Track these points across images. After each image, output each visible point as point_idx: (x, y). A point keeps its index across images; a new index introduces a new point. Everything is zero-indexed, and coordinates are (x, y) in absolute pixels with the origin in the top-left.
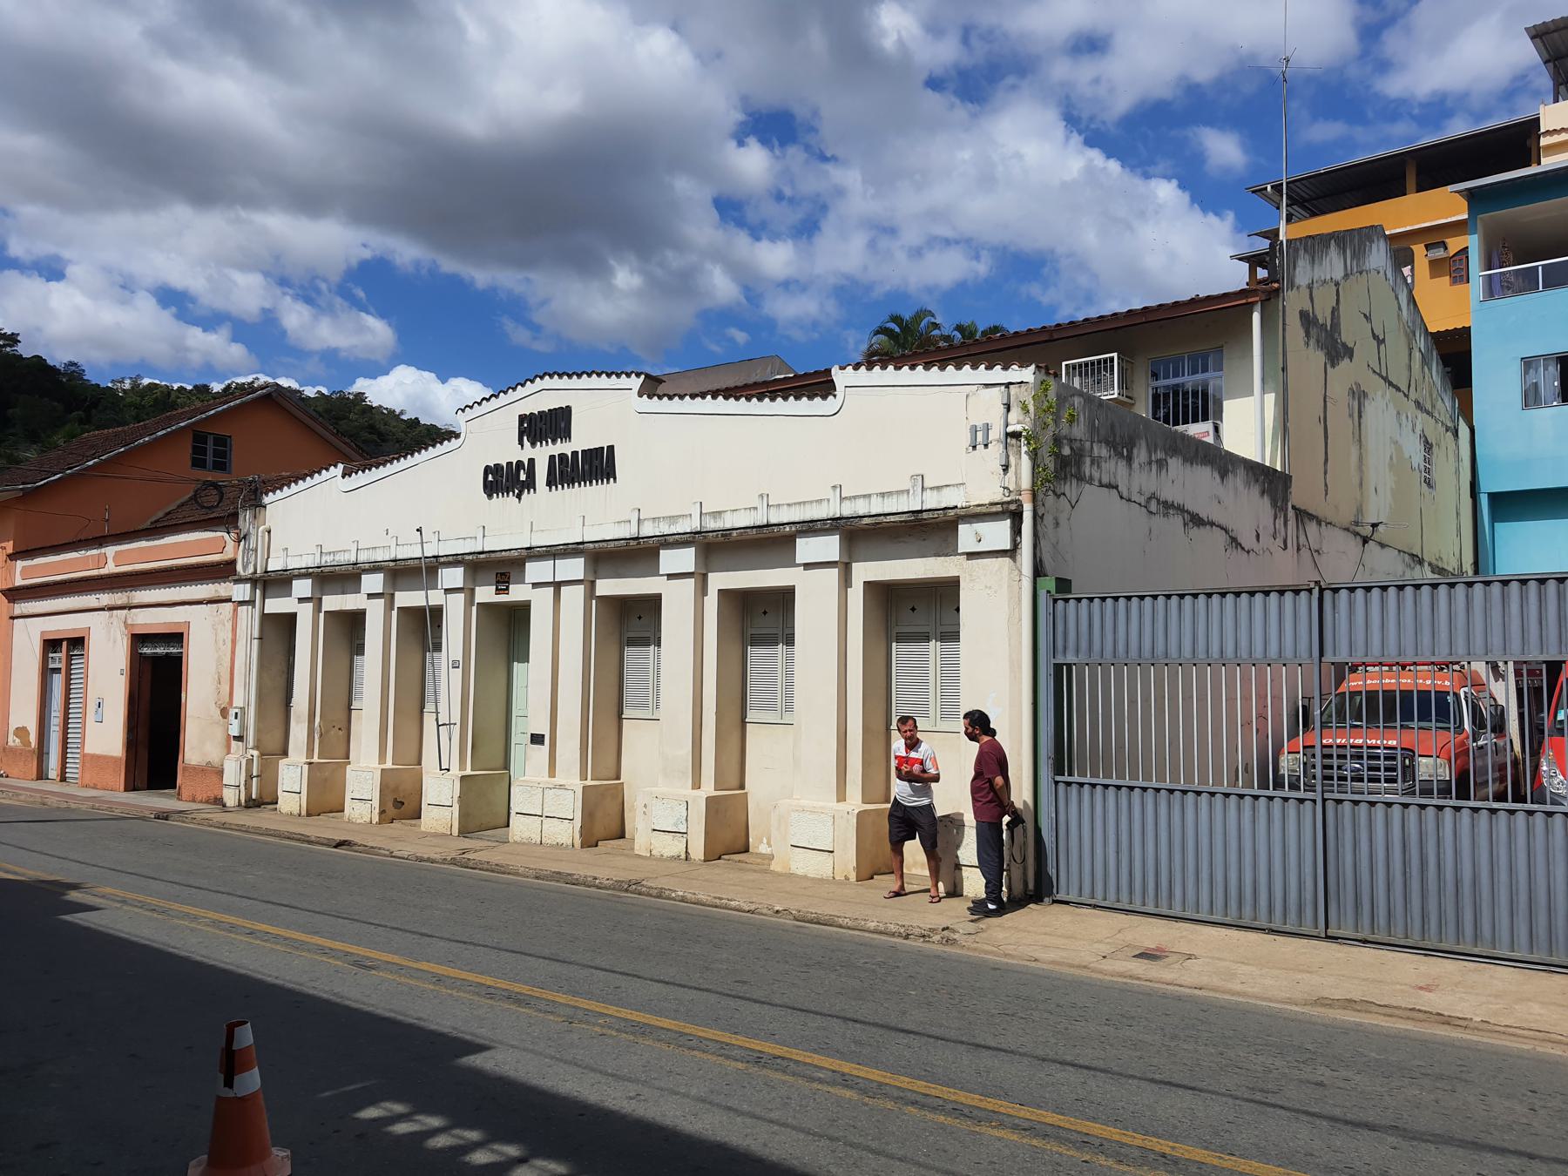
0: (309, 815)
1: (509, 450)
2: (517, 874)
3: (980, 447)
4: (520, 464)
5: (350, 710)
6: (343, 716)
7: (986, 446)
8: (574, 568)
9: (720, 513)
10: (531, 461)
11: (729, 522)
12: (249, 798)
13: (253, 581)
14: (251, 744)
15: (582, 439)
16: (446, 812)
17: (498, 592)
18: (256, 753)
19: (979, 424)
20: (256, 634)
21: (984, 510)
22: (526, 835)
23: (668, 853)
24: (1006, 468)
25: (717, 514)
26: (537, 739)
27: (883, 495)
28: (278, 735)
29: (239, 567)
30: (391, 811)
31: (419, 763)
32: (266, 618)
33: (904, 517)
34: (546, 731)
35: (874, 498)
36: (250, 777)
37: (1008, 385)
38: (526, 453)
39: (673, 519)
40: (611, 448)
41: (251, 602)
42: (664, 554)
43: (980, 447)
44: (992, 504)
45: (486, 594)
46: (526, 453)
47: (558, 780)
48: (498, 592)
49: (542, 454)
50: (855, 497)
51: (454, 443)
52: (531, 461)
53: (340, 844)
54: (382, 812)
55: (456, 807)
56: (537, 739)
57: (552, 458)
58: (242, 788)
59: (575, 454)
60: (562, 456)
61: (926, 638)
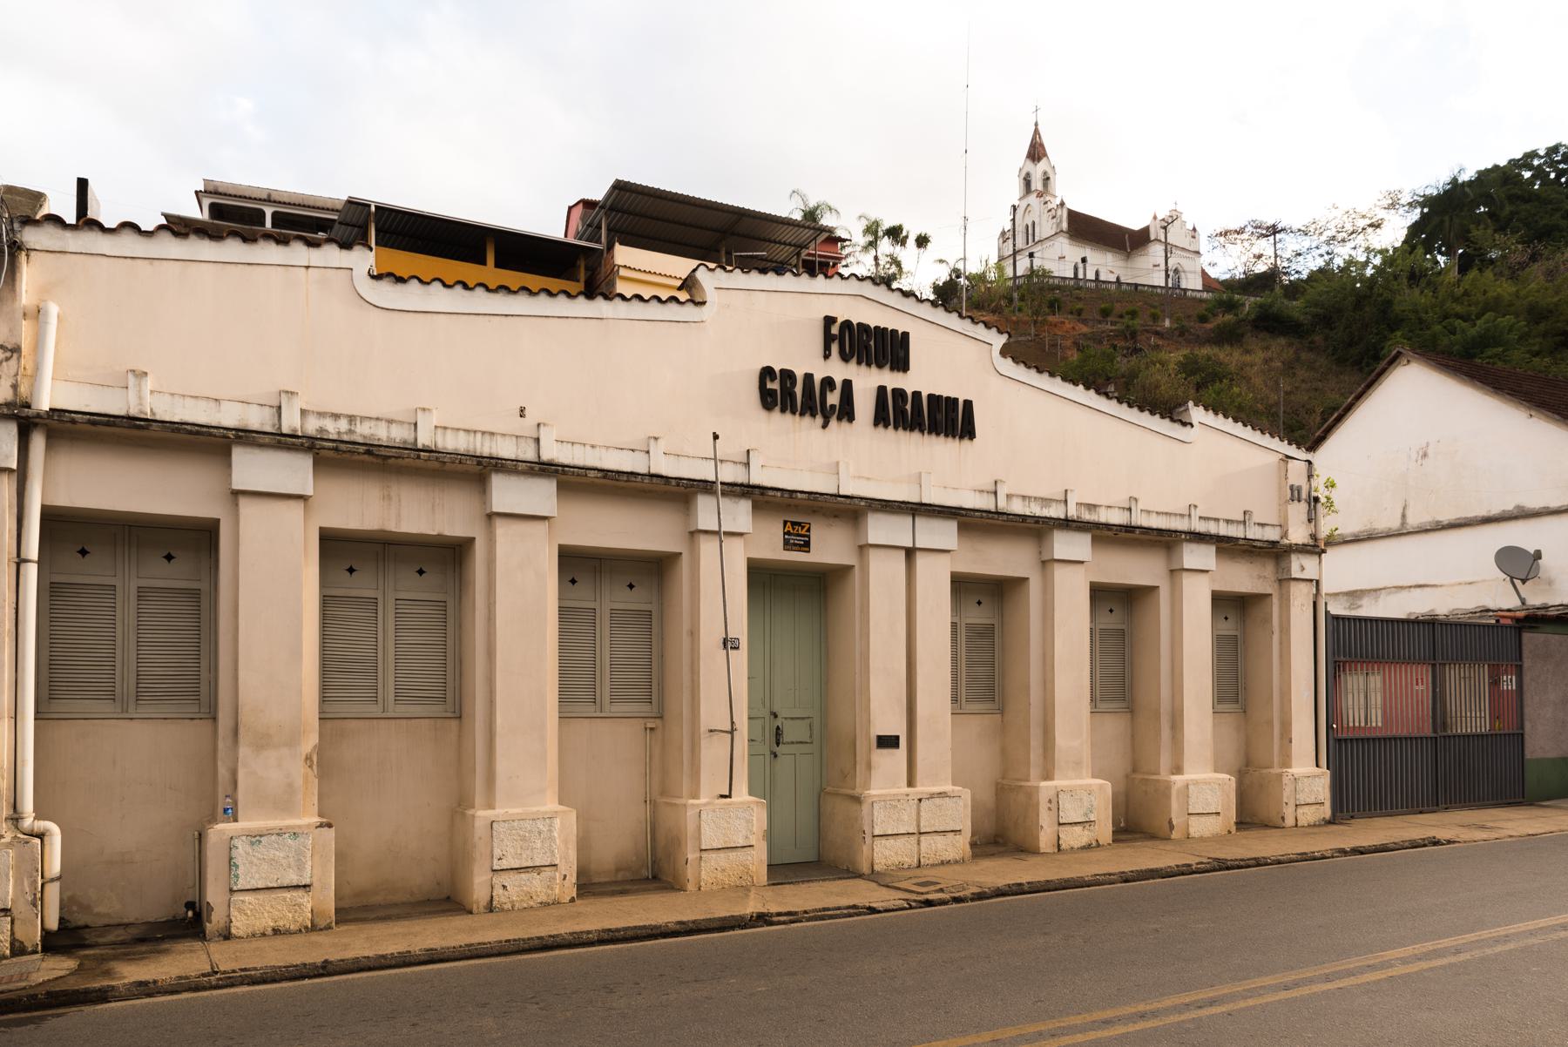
4: (828, 383)
10: (847, 384)
15: (926, 375)
17: (788, 545)
24: (1310, 521)
25: (1092, 507)
27: (1228, 521)
38: (838, 370)
39: (1046, 501)
40: (968, 404)
45: (769, 544)
48: (788, 545)
49: (867, 381)
57: (882, 390)
59: (917, 395)
60: (899, 394)
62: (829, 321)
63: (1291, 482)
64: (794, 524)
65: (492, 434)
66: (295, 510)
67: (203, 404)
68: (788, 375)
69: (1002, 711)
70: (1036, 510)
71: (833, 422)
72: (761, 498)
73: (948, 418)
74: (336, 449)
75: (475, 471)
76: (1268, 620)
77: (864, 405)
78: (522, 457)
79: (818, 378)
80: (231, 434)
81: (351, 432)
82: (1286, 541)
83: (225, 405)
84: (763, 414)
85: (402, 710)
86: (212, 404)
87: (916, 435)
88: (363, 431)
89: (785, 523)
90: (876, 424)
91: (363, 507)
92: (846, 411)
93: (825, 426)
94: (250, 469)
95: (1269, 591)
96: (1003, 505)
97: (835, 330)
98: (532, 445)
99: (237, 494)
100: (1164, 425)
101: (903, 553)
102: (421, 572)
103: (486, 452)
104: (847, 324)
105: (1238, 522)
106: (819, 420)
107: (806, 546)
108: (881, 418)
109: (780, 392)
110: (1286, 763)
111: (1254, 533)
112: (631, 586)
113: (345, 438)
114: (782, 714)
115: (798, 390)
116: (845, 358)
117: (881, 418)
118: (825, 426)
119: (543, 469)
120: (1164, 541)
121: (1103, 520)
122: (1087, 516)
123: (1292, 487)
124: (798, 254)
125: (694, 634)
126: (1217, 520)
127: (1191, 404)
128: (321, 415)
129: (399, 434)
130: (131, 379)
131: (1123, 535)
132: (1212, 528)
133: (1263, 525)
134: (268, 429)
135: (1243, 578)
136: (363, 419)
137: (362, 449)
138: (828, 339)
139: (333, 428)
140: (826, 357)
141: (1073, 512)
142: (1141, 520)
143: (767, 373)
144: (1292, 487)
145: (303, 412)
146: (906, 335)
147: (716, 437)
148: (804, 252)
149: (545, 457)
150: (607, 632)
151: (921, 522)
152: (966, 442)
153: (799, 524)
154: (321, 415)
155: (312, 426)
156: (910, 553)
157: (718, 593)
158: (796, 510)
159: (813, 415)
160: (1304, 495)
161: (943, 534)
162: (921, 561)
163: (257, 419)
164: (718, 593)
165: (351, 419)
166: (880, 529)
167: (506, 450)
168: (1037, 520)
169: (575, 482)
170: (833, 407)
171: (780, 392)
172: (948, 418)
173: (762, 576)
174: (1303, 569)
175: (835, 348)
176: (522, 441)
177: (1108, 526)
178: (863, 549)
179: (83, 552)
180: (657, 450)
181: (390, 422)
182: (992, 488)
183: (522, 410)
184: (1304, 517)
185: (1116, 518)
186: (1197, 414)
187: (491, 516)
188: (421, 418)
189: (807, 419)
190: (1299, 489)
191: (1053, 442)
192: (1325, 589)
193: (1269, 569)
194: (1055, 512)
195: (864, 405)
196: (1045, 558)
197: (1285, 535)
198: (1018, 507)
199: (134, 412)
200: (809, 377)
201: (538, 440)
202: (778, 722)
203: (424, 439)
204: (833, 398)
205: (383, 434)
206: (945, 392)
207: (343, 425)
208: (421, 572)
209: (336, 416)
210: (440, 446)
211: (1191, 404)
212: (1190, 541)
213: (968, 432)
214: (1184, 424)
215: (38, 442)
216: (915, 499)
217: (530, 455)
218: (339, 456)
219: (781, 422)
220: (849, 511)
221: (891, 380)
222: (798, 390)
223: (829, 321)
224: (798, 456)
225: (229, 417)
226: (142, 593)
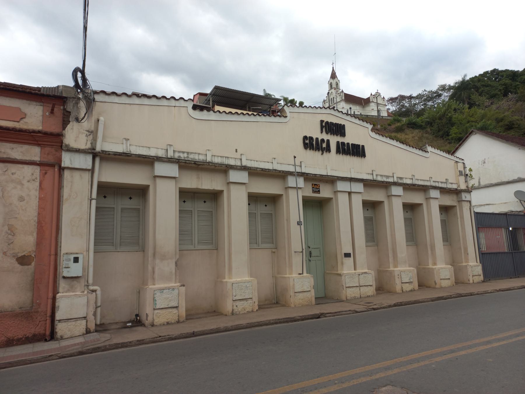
0: (187, 319)
4: (323, 140)
10: (328, 141)
13: (95, 154)
17: (314, 192)
22: (353, 295)
24: (466, 182)
25: (401, 178)
26: (347, 255)
27: (442, 182)
34: (350, 251)
38: (325, 137)
39: (388, 177)
40: (363, 146)
45: (309, 193)
49: (334, 140)
51: (282, 119)
55: (313, 292)
56: (347, 255)
58: (91, 317)
59: (348, 144)
60: (343, 143)
62: (322, 121)
64: (315, 185)
65: (228, 157)
66: (173, 182)
67: (145, 149)
68: (311, 138)
69: (377, 245)
70: (385, 179)
71: (325, 153)
72: (307, 177)
73: (358, 151)
74: (185, 163)
75: (224, 169)
76: (456, 214)
78: (237, 165)
79: (320, 139)
80: (155, 158)
81: (188, 157)
82: (459, 188)
83: (152, 149)
84: (304, 150)
85: (200, 247)
86: (148, 149)
87: (348, 157)
88: (191, 156)
90: (337, 153)
91: (192, 181)
92: (328, 149)
93: (322, 154)
94: (160, 169)
95: (455, 205)
96: (375, 177)
97: (324, 124)
98: (240, 161)
99: (155, 177)
100: (420, 152)
101: (347, 194)
102: (205, 202)
103: (226, 163)
104: (327, 122)
105: (444, 183)
106: (321, 152)
107: (319, 192)
108: (338, 151)
109: (309, 144)
110: (467, 261)
111: (449, 186)
112: (266, 206)
113: (186, 159)
114: (311, 247)
115: (314, 143)
116: (327, 133)
117: (338, 151)
118: (322, 154)
119: (244, 168)
120: (424, 189)
121: (405, 182)
122: (400, 181)
123: (460, 171)
124: (270, 108)
125: (288, 220)
126: (438, 182)
127: (427, 145)
128: (179, 152)
129: (202, 158)
130: (124, 141)
131: (411, 187)
132: (437, 185)
134: (164, 156)
135: (448, 201)
136: (191, 153)
137: (193, 162)
139: (183, 156)
140: (322, 132)
141: (396, 180)
143: (305, 138)
145: (174, 151)
146: (344, 125)
147: (295, 157)
148: (272, 107)
149: (244, 164)
150: (259, 220)
151: (352, 184)
152: (363, 158)
154: (179, 152)
155: (177, 155)
157: (293, 207)
158: (315, 180)
159: (319, 151)
161: (359, 187)
162: (353, 196)
163: (161, 153)
164: (293, 207)
165: (188, 153)
166: (341, 186)
167: (232, 162)
168: (387, 182)
169: (255, 173)
171: (309, 144)
172: (358, 151)
173: (307, 203)
174: (466, 197)
176: (237, 160)
177: (408, 184)
178: (336, 192)
179: (105, 197)
180: (275, 162)
181: (199, 154)
182: (371, 173)
183: (236, 150)
184: (464, 181)
185: (409, 182)
186: (429, 149)
187: (229, 183)
188: (208, 153)
189: (317, 152)
191: (391, 159)
192: (473, 204)
193: (455, 197)
194: (391, 180)
196: (389, 194)
197: (459, 186)
198: (379, 179)
199: (125, 151)
200: (317, 139)
201: (241, 159)
202: (310, 250)
203: (209, 159)
204: (324, 145)
205: (196, 157)
207: (185, 155)
208: (205, 202)
209: (183, 152)
210: (213, 161)
211: (427, 145)
212: (432, 188)
214: (426, 152)
215: (97, 160)
216: (349, 176)
217: (239, 164)
218: (187, 165)
220: (331, 180)
221: (340, 139)
222: (314, 143)
223: (322, 121)
225: (152, 153)
226: (123, 210)
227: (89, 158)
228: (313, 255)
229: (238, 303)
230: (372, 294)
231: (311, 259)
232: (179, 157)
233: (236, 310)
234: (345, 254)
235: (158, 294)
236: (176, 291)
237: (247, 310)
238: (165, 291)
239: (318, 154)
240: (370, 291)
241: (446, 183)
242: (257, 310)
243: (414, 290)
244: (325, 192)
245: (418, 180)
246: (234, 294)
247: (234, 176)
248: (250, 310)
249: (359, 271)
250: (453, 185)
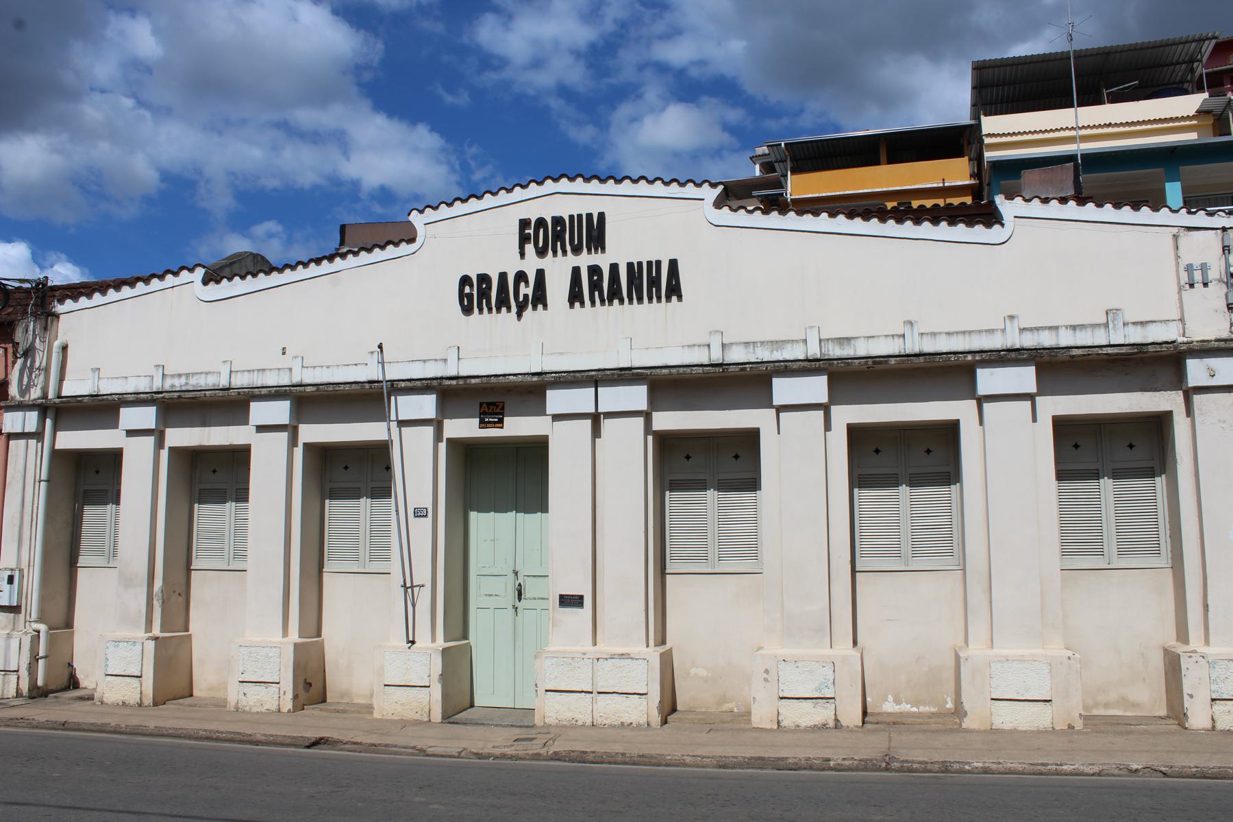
0: (155, 704)
1: (500, 256)
2: (685, 765)
3: (1199, 286)
4: (521, 277)
5: (189, 570)
6: (183, 581)
7: (1205, 285)
8: (637, 397)
9: (848, 339)
10: (540, 274)
11: (862, 349)
12: (33, 686)
13: (43, 408)
14: (34, 616)
15: (621, 250)
16: (422, 694)
18: (42, 627)
19: (1197, 263)
20: (44, 476)
21: (1222, 344)
22: (568, 715)
23: (805, 722)
26: (570, 601)
27: (1074, 328)
28: (61, 603)
29: (13, 390)
30: (303, 695)
31: (319, 634)
32: (58, 456)
33: (1124, 350)
35: (1062, 331)
36: (35, 658)
37: (1224, 229)
38: (531, 264)
40: (673, 264)
41: (38, 435)
42: (124, 412)
43: (1199, 286)
44: (1218, 340)
45: (465, 427)
46: (531, 264)
47: (600, 646)
48: (483, 424)
49: (558, 270)
50: (1038, 329)
51: (404, 248)
52: (540, 274)
53: (317, 743)
54: (296, 697)
56: (570, 601)
57: (576, 271)
58: (24, 673)
60: (594, 270)
61: (1096, 475)
62: (524, 224)
63: (1184, 261)
64: (489, 404)
65: (264, 370)
68: (484, 279)
73: (656, 282)
77: (558, 288)
81: (187, 384)
89: (481, 404)
90: (572, 305)
92: (540, 298)
100: (979, 232)
104: (541, 222)
108: (575, 296)
109: (479, 294)
121: (862, 352)
122: (836, 352)
123: (1189, 269)
128: (173, 376)
132: (1047, 340)
133: (1142, 324)
138: (524, 239)
140: (522, 255)
141: (814, 351)
142: (913, 345)
143: (465, 280)
144: (1189, 269)
146: (602, 216)
153: (493, 404)
154: (173, 376)
156: (596, 419)
160: (1213, 274)
162: (607, 425)
163: (143, 385)
165: (187, 375)
170: (526, 296)
171: (479, 294)
172: (656, 282)
175: (530, 248)
190: (1204, 268)
195: (558, 288)
198: (737, 355)
200: (503, 277)
204: (527, 290)
206: (643, 255)
209: (180, 375)
213: (674, 290)
219: (481, 320)
221: (585, 260)
223: (524, 224)
224: (499, 347)
225: (129, 387)
227: (33, 416)
228: (527, 593)
229: (249, 688)
230: (643, 720)
231: (518, 604)
232: (173, 386)
233: (244, 703)
234: (561, 596)
235: (111, 648)
236: (139, 647)
237: (267, 707)
238: (121, 644)
239: (507, 318)
240: (643, 710)
241: (1106, 325)
242: (289, 711)
243: (838, 725)
244: (517, 426)
245: (934, 334)
246: (241, 669)
247: (261, 412)
248: (274, 708)
249: (604, 647)
250: (1151, 327)
